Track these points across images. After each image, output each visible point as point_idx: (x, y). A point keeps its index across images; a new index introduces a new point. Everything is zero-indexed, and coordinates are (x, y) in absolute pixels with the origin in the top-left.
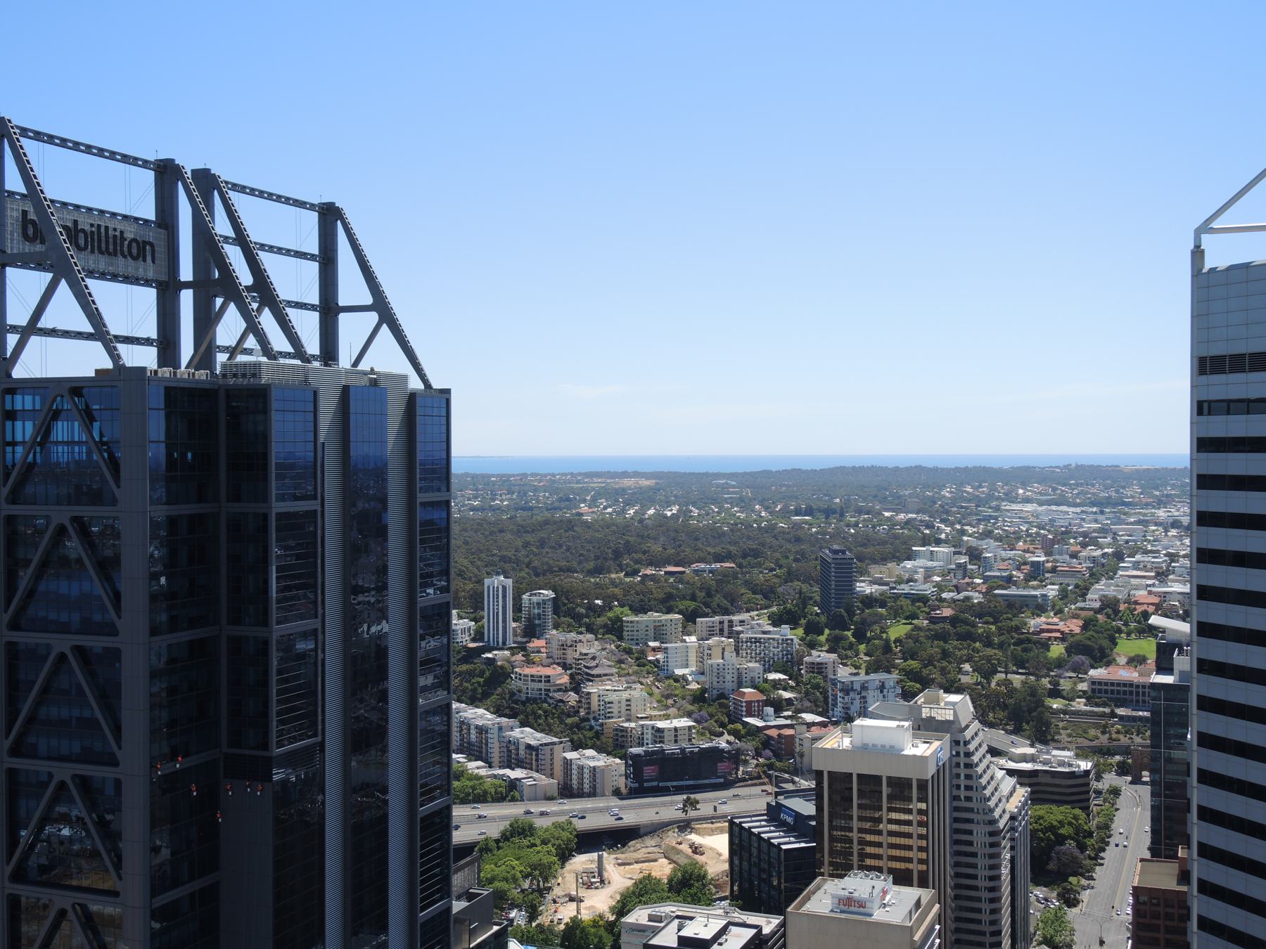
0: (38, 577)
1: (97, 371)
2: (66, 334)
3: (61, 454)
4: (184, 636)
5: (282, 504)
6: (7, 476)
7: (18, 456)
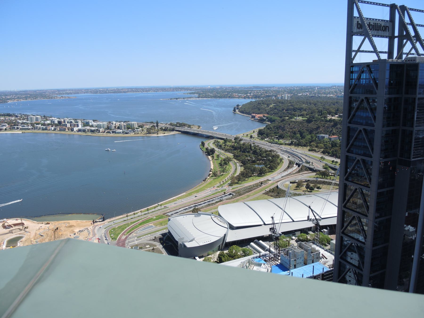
0: (356, 111)
1: (373, 61)
2: (366, 52)
3: (363, 82)
4: (391, 128)
5: (420, 95)
6: (350, 87)
7: (353, 82)
